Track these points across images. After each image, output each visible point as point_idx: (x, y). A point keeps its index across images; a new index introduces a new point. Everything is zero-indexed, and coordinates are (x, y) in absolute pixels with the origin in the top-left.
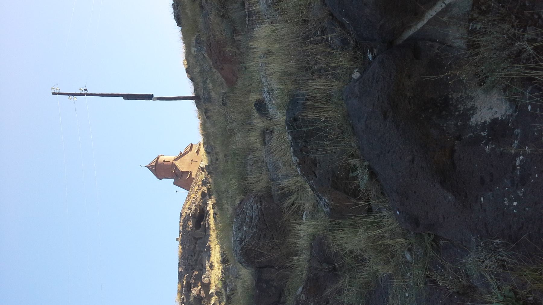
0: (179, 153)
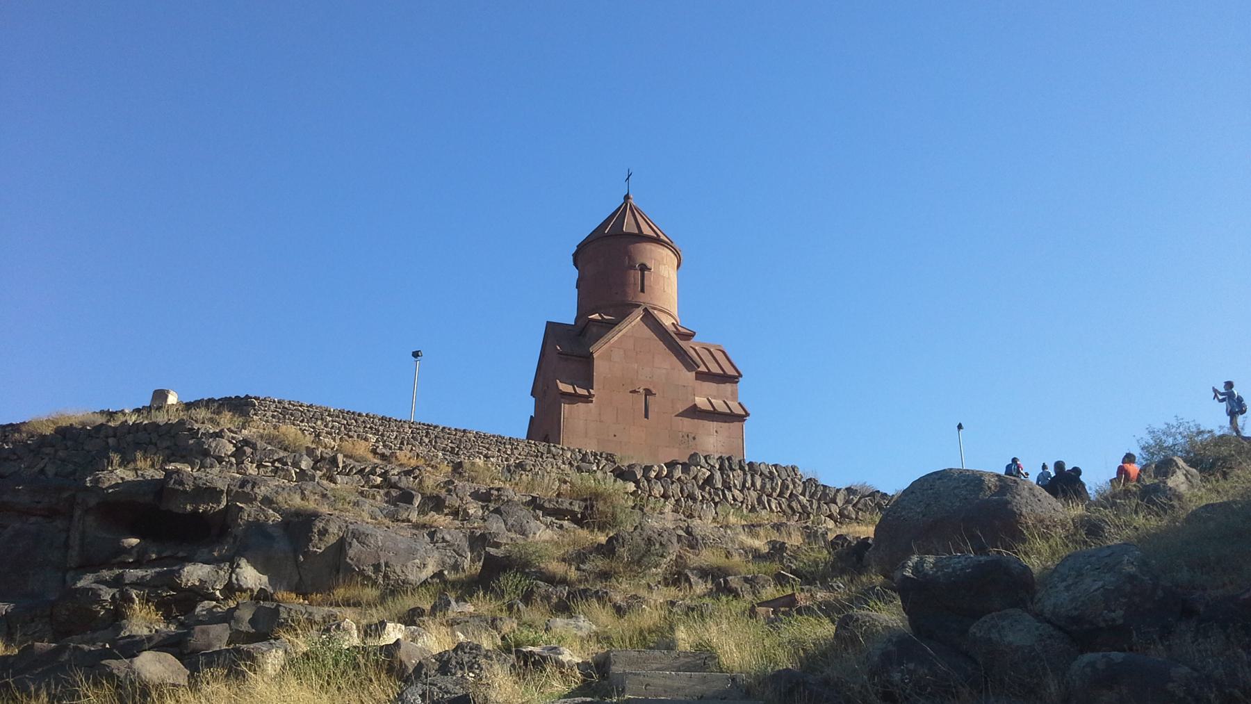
0: (687, 325)
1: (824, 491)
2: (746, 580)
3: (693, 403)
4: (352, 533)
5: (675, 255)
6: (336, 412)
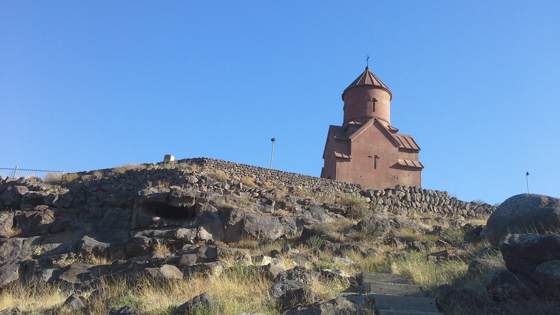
0: (394, 126)
1: (460, 203)
2: (423, 243)
4: (247, 217)
5: (389, 94)
6: (239, 165)
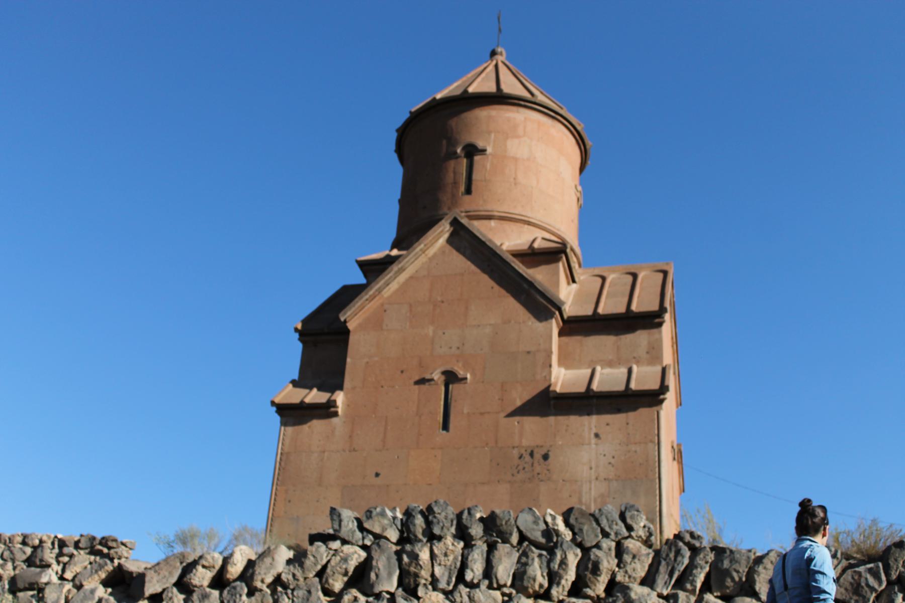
1: (714, 566)
3: (546, 385)
